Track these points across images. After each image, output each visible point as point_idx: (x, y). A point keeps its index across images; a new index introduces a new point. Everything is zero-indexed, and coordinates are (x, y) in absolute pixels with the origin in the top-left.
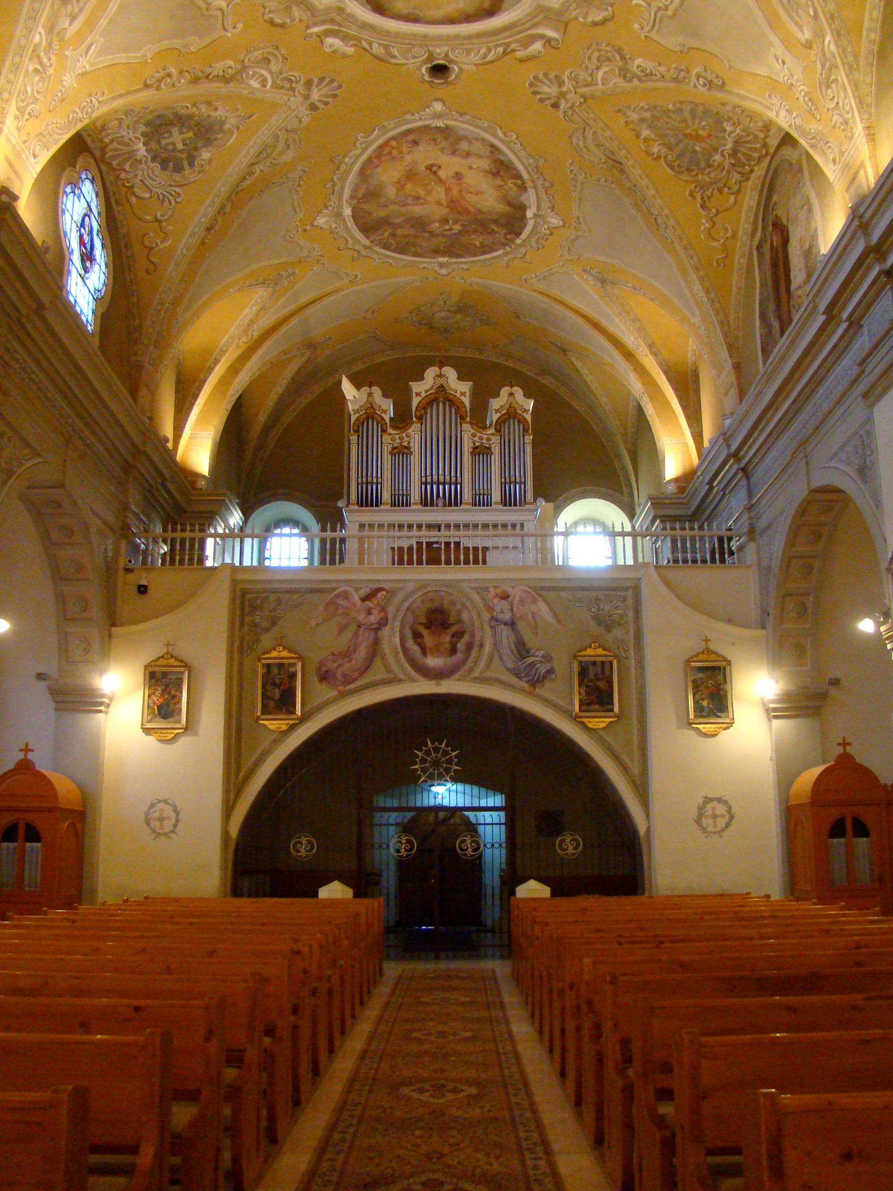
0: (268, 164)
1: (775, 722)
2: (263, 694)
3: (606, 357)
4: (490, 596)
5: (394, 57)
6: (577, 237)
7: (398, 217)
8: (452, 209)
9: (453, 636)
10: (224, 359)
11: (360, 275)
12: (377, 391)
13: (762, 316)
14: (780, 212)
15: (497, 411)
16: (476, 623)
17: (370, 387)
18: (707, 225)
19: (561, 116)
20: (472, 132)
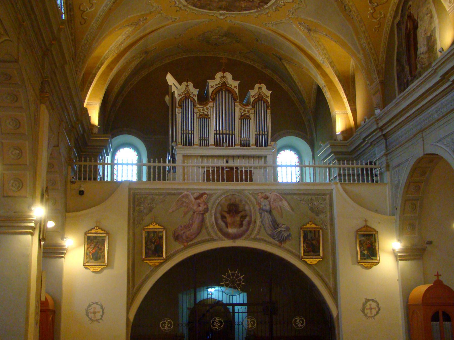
1: (401, 263)
2: (146, 247)
3: (304, 65)
4: (259, 197)
6: (298, 8)
11: (178, 19)
12: (191, 85)
13: (398, 60)
14: (413, 11)
15: (253, 97)
16: (253, 211)
17: (187, 82)
18: (371, 11)
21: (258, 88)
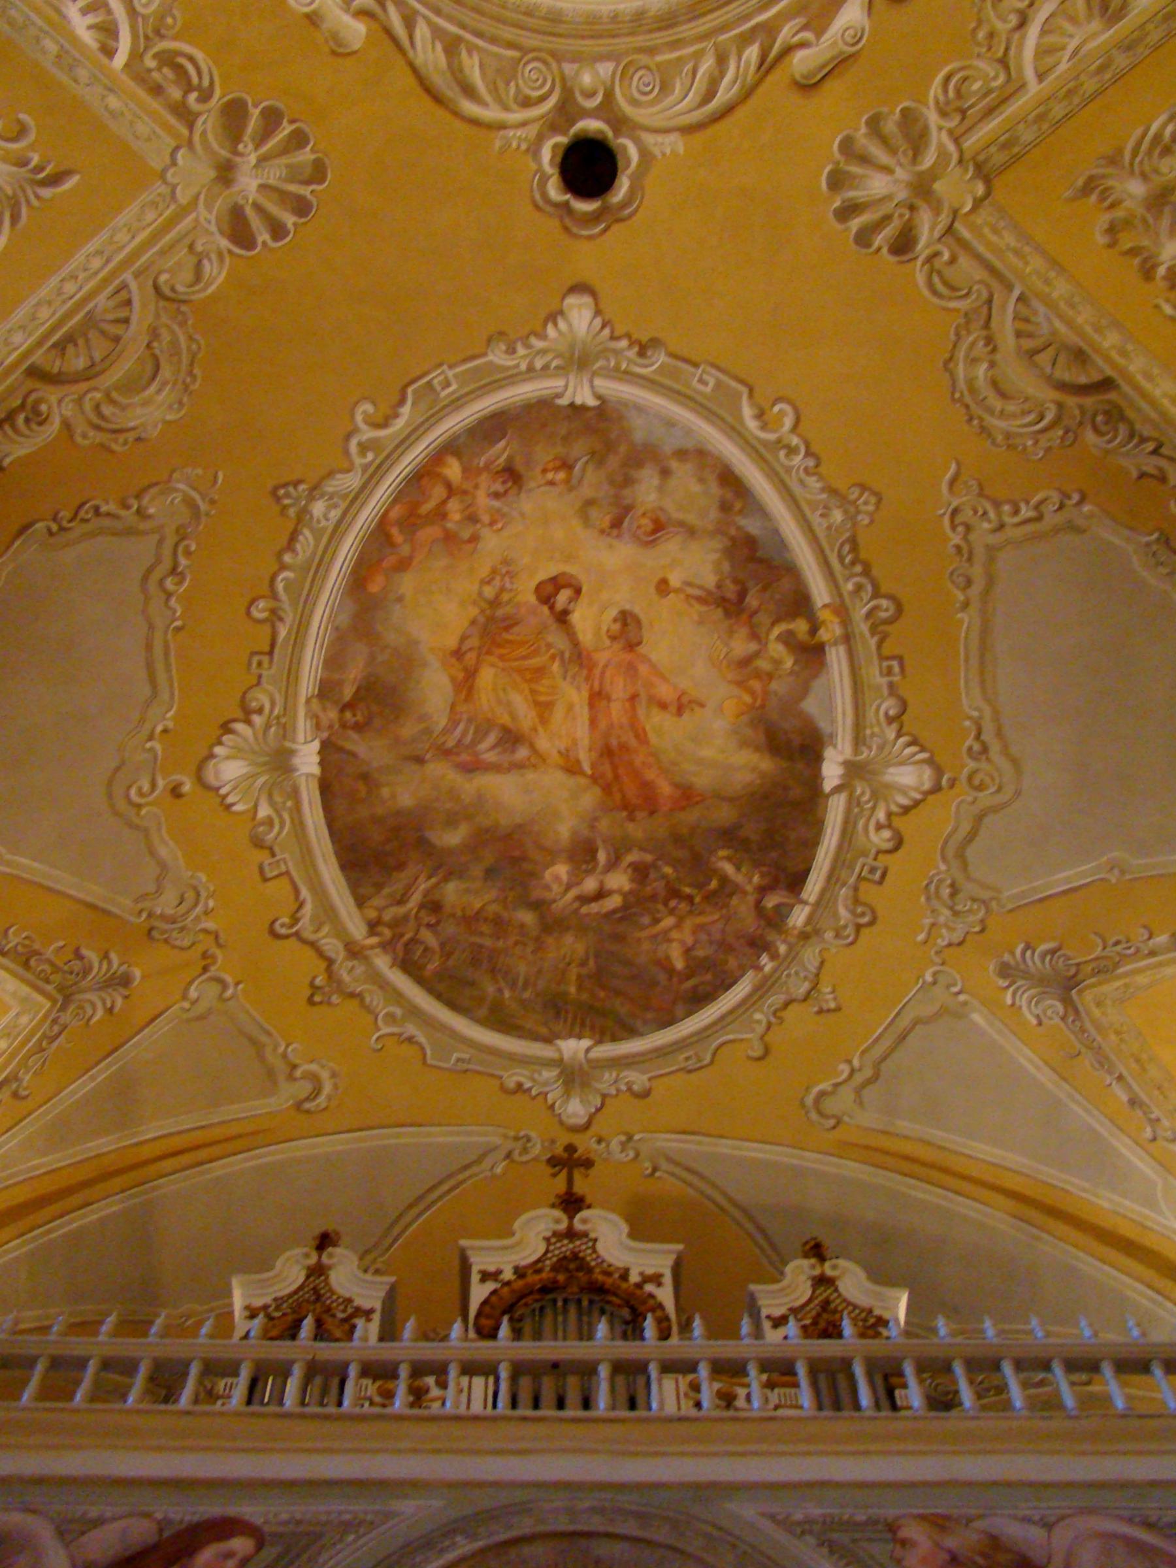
0: (88, 406)
5: (469, 91)
6: (979, 818)
7: (452, 821)
8: (607, 789)
11: (327, 1088)
19: (920, 278)
20: (670, 424)
21: (809, 1283)
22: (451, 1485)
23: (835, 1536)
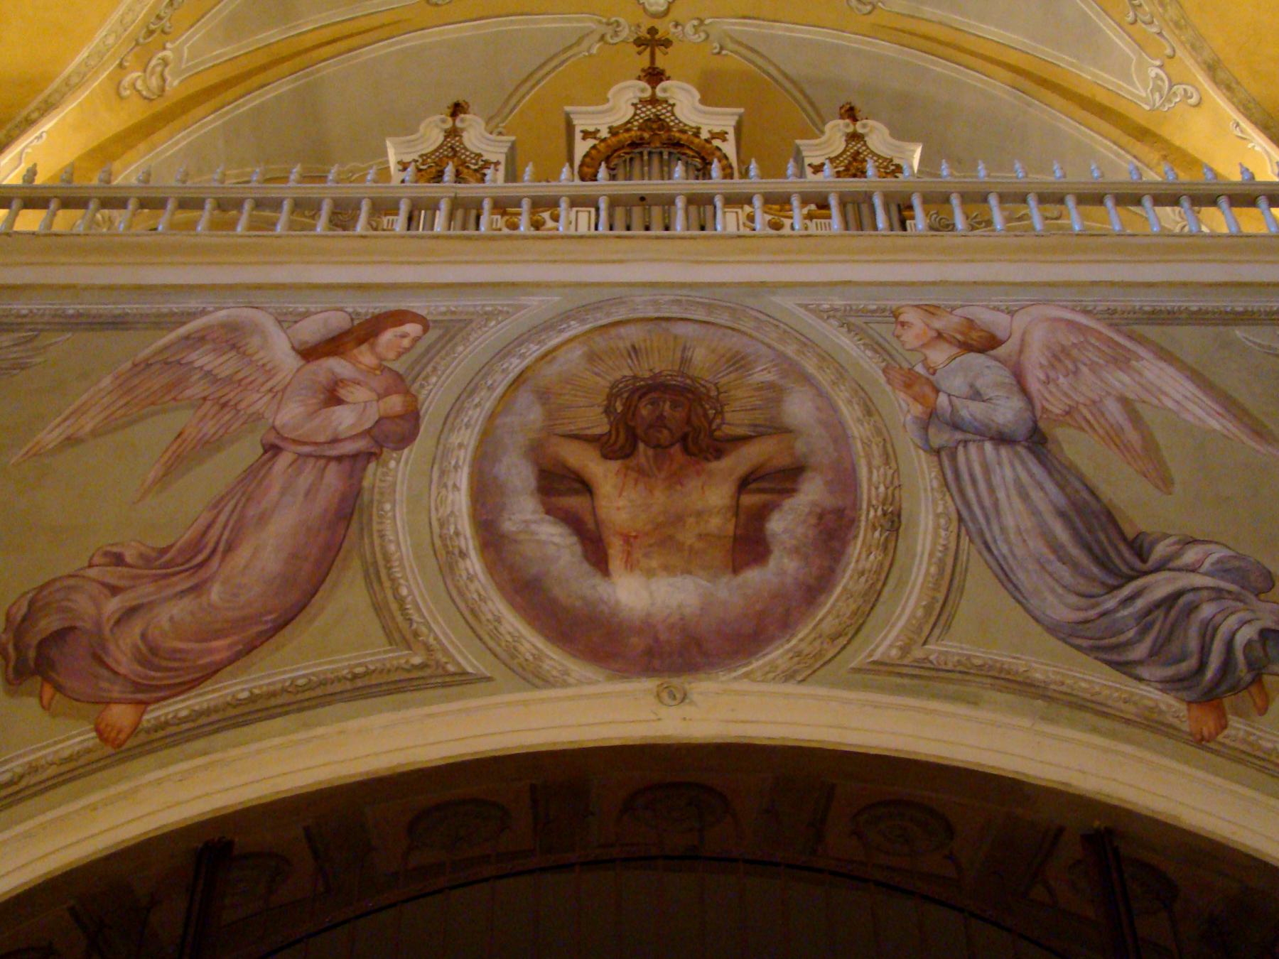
4: (910, 338)
9: (744, 484)
10: (69, 109)
16: (858, 430)
21: (844, 138)
22: (564, 285)
23: (852, 320)
